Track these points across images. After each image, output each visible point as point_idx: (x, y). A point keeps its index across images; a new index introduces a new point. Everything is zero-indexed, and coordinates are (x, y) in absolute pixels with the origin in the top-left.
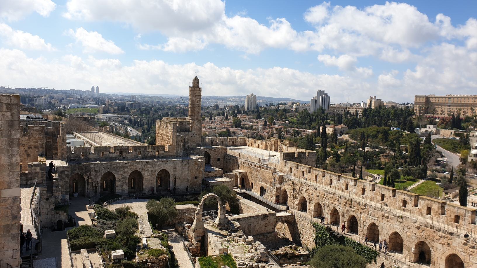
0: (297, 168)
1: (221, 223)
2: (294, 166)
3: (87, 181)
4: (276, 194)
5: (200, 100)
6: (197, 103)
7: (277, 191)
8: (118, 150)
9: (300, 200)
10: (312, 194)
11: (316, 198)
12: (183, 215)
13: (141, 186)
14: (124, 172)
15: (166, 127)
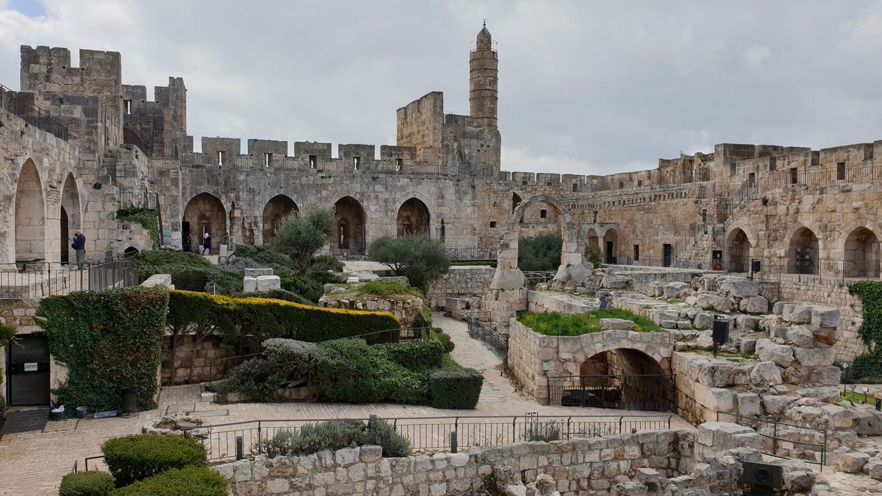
0: (773, 167)
1: (573, 276)
2: (761, 165)
3: (230, 213)
4: (712, 247)
5: (495, 80)
6: (489, 88)
7: (714, 239)
8: (307, 151)
9: (792, 243)
10: (834, 211)
11: (851, 216)
12: (464, 285)
13: (362, 242)
14: (320, 200)
15: (419, 111)
